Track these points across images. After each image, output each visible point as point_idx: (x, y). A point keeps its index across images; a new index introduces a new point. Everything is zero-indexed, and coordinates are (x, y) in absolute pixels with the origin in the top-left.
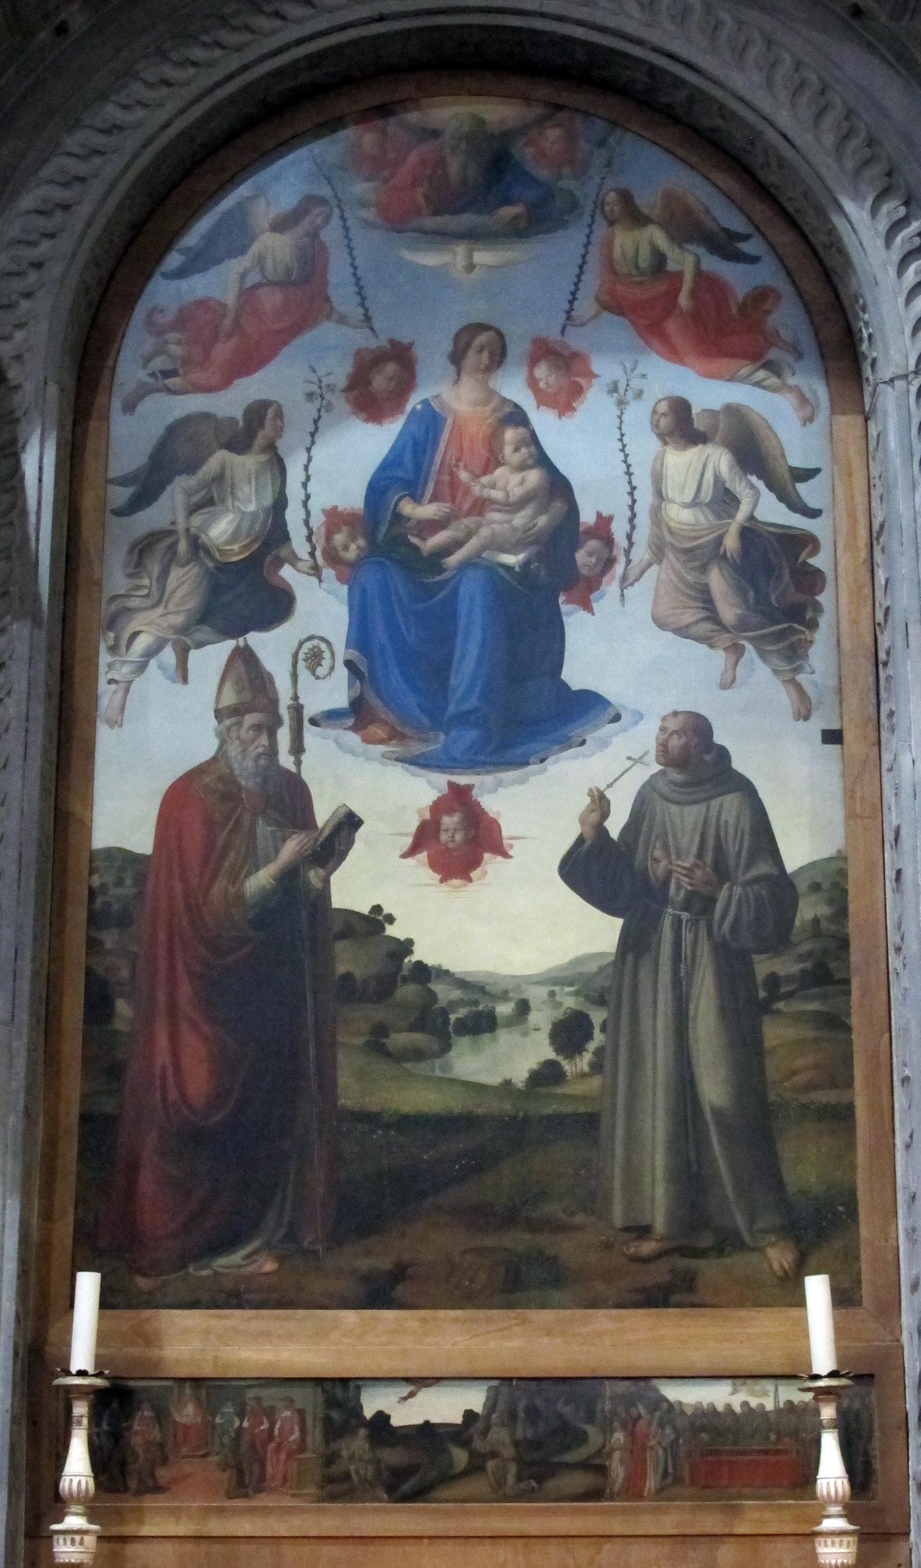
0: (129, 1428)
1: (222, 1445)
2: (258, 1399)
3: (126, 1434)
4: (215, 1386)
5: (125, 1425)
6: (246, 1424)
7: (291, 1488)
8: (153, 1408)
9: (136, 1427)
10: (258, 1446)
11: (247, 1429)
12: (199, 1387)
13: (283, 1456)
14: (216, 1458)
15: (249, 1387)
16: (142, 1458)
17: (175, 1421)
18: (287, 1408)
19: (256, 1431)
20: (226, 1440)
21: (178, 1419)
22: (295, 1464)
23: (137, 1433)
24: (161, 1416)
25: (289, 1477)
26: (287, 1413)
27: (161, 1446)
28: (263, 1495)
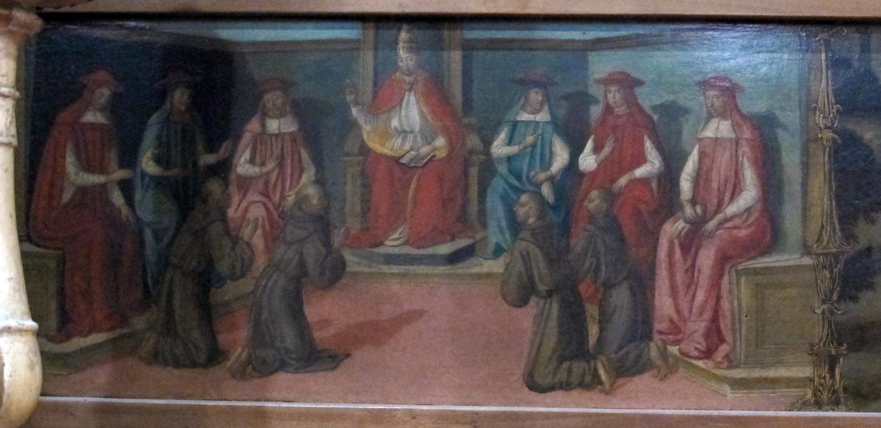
0: (222, 170)
1: (515, 226)
2: (628, 83)
3: (214, 187)
4: (492, 45)
5: (209, 159)
6: (588, 161)
7: (730, 362)
8: (301, 110)
9: (243, 166)
10: (629, 229)
11: (594, 174)
12: (438, 46)
13: (706, 258)
14: (496, 266)
15: (599, 44)
16: (261, 262)
17: (365, 150)
18: (723, 115)
19: (623, 181)
20: (526, 208)
21: (375, 145)
22: (745, 292)
23: (245, 183)
24: (321, 128)
25: (725, 325)
26: (720, 128)
27: (323, 224)
28: (644, 382)
